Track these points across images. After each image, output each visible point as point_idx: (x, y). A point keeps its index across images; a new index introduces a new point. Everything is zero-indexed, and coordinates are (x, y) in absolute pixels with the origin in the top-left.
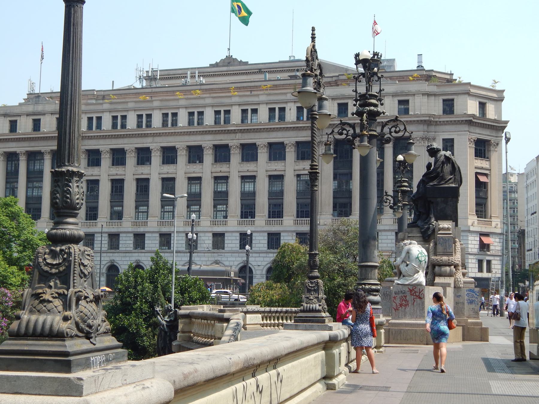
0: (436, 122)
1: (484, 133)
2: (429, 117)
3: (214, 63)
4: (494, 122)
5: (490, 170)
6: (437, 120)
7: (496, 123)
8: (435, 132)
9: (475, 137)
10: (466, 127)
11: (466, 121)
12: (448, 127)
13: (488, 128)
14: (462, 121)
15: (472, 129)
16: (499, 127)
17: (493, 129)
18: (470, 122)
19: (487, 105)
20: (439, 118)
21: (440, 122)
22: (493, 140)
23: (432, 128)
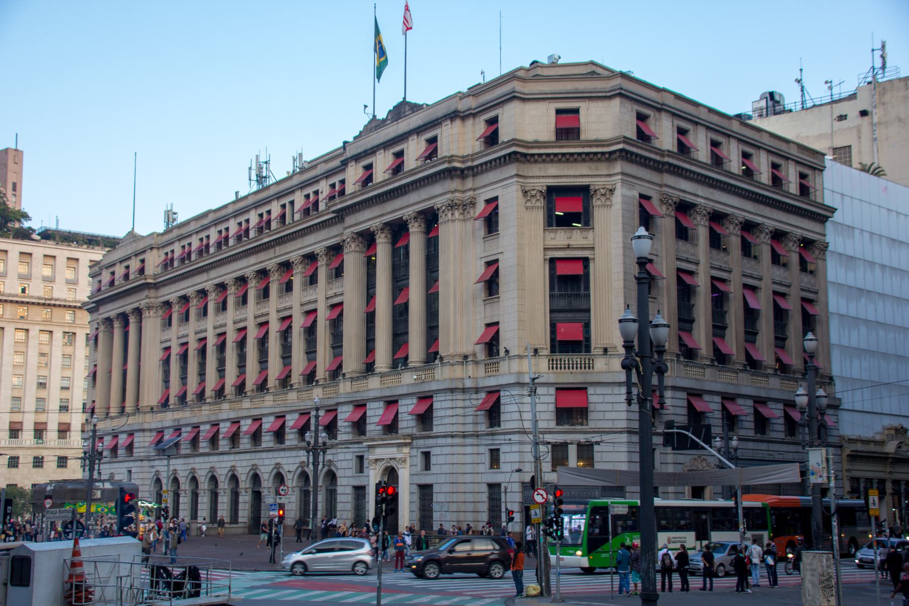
0: (471, 168)
1: (571, 173)
2: (449, 162)
3: (357, 133)
4: (590, 146)
5: (593, 248)
6: (469, 164)
7: (597, 146)
8: (474, 190)
9: (541, 184)
10: (512, 169)
11: (510, 154)
12: (492, 176)
13: (584, 161)
14: (504, 156)
15: (535, 170)
16: (611, 153)
17: (599, 160)
18: (521, 156)
19: (582, 113)
20: (473, 160)
21: (477, 166)
22: (596, 183)
23: (469, 183)
